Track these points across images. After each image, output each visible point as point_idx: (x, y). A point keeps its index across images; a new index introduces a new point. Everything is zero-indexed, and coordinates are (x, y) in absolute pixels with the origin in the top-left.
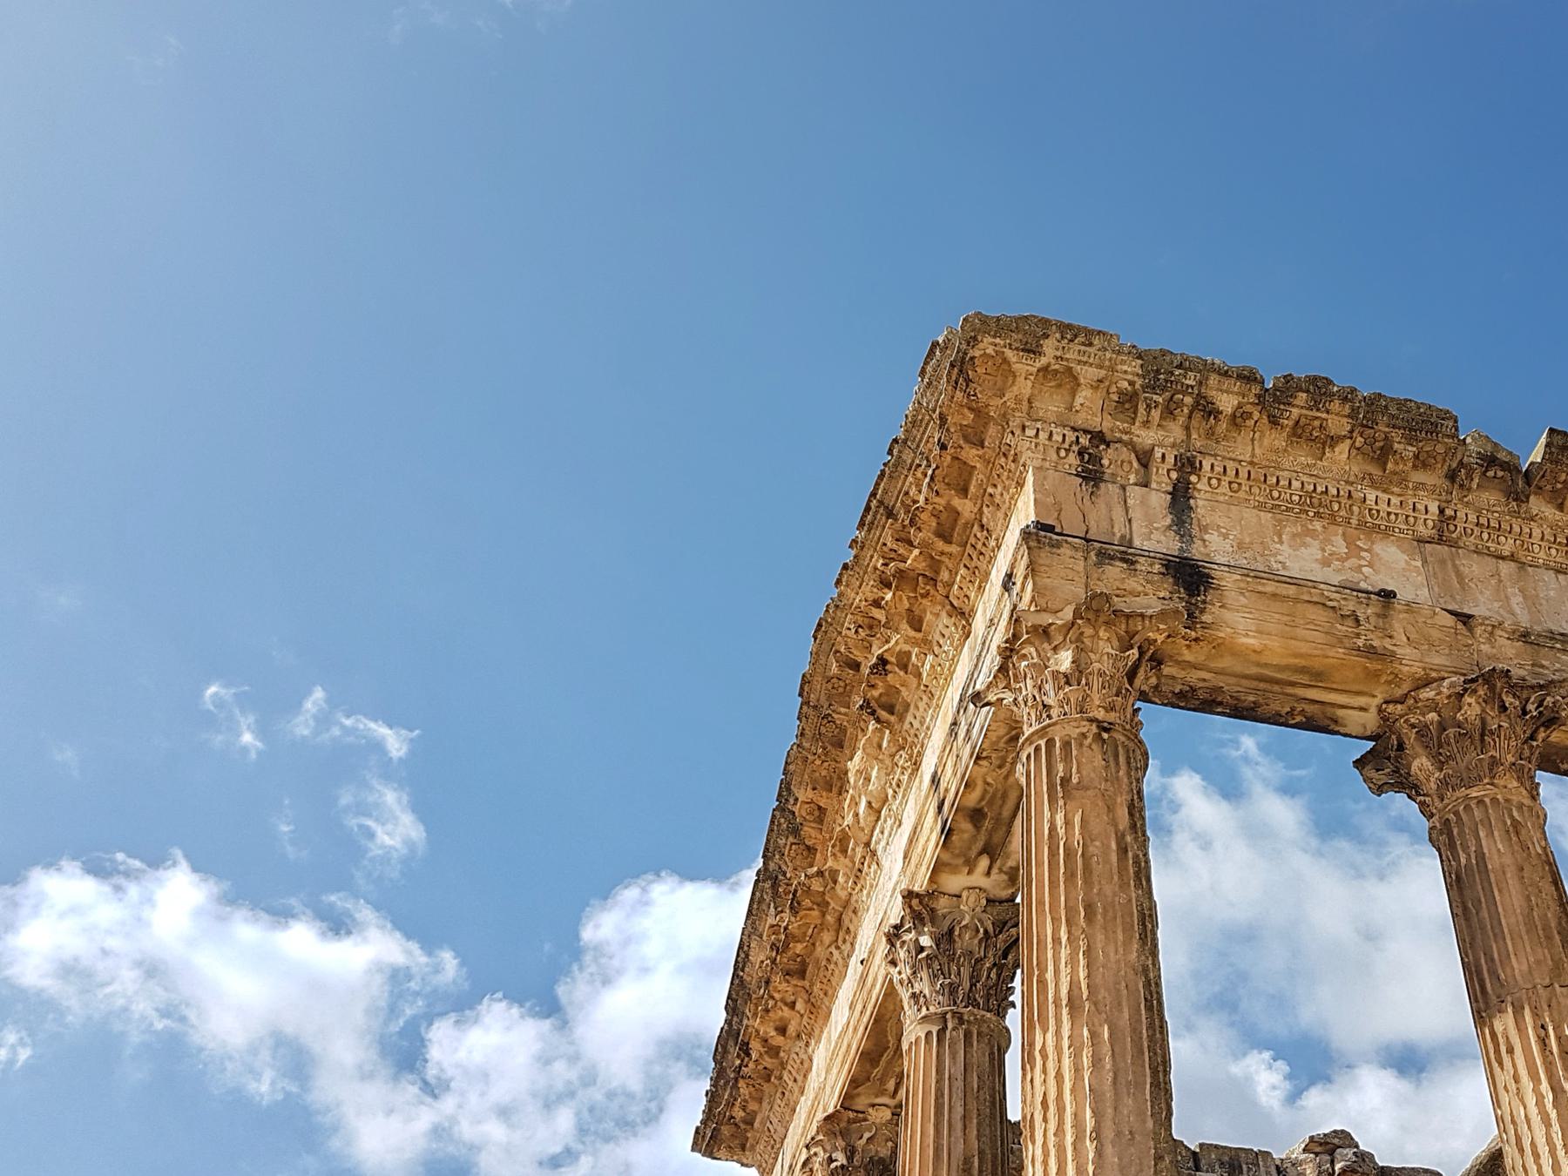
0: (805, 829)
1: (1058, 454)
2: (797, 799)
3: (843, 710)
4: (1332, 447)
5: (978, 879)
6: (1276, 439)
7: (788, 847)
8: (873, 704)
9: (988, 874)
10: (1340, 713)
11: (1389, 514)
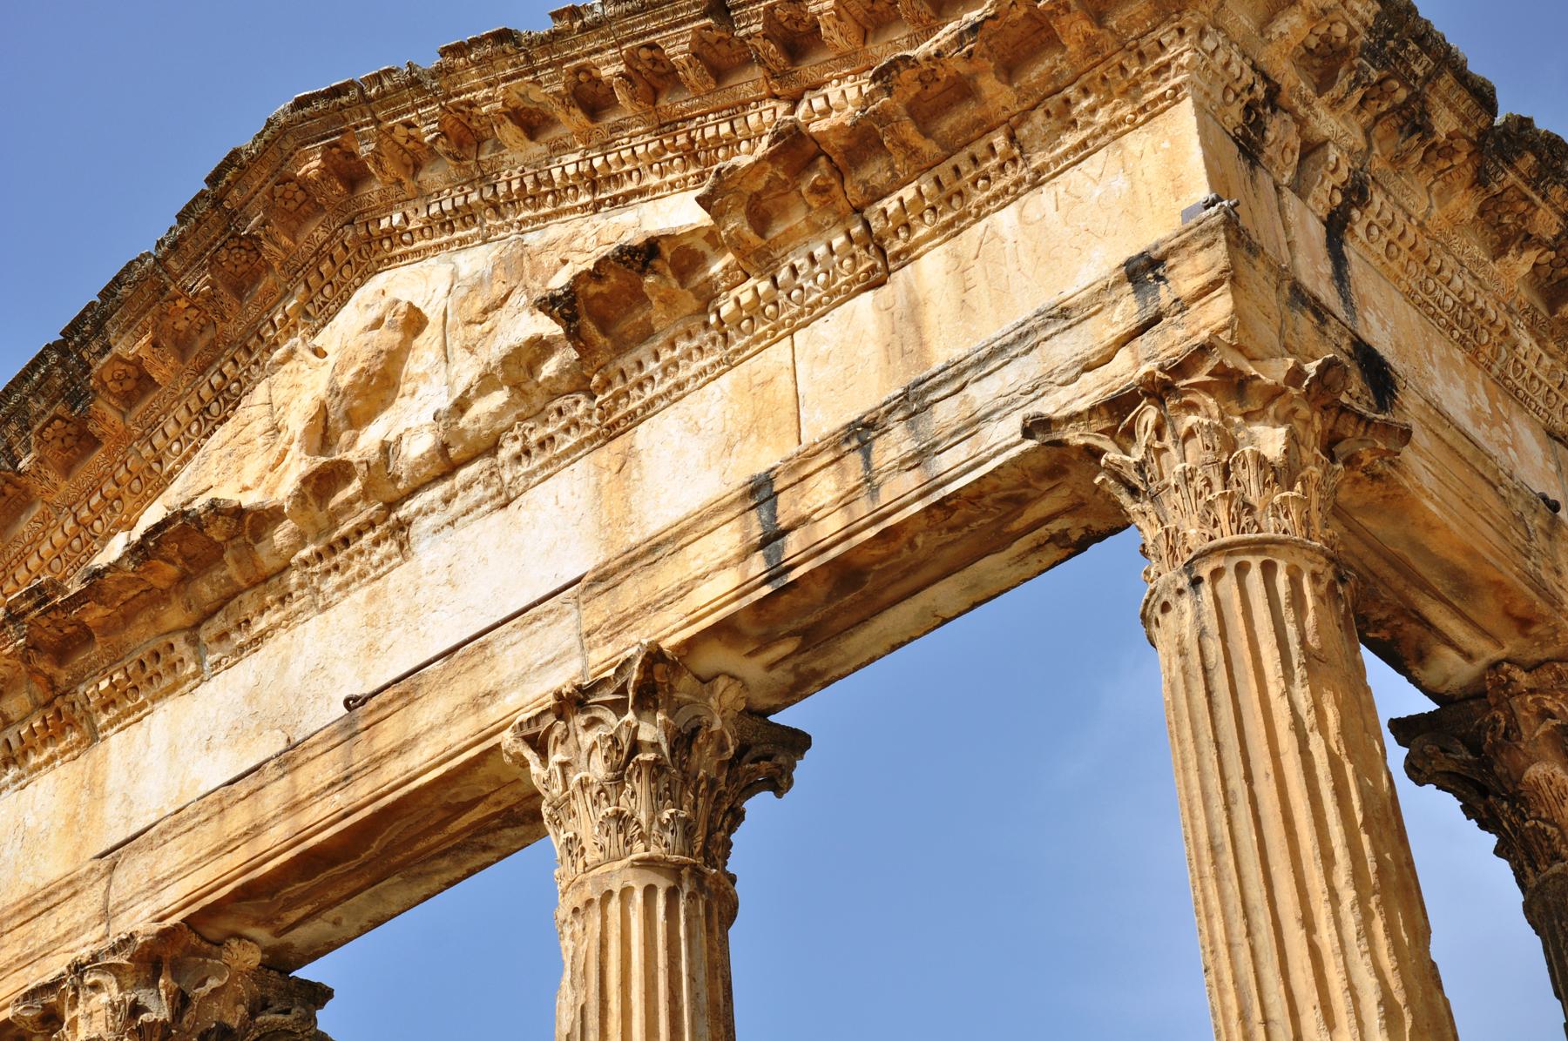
0: (100, 403)
1: (1224, 95)
2: (107, 348)
3: (285, 241)
4: (1522, 249)
5: (752, 669)
6: (1465, 204)
7: (45, 420)
8: (580, 304)
9: (771, 666)
11: (1533, 377)
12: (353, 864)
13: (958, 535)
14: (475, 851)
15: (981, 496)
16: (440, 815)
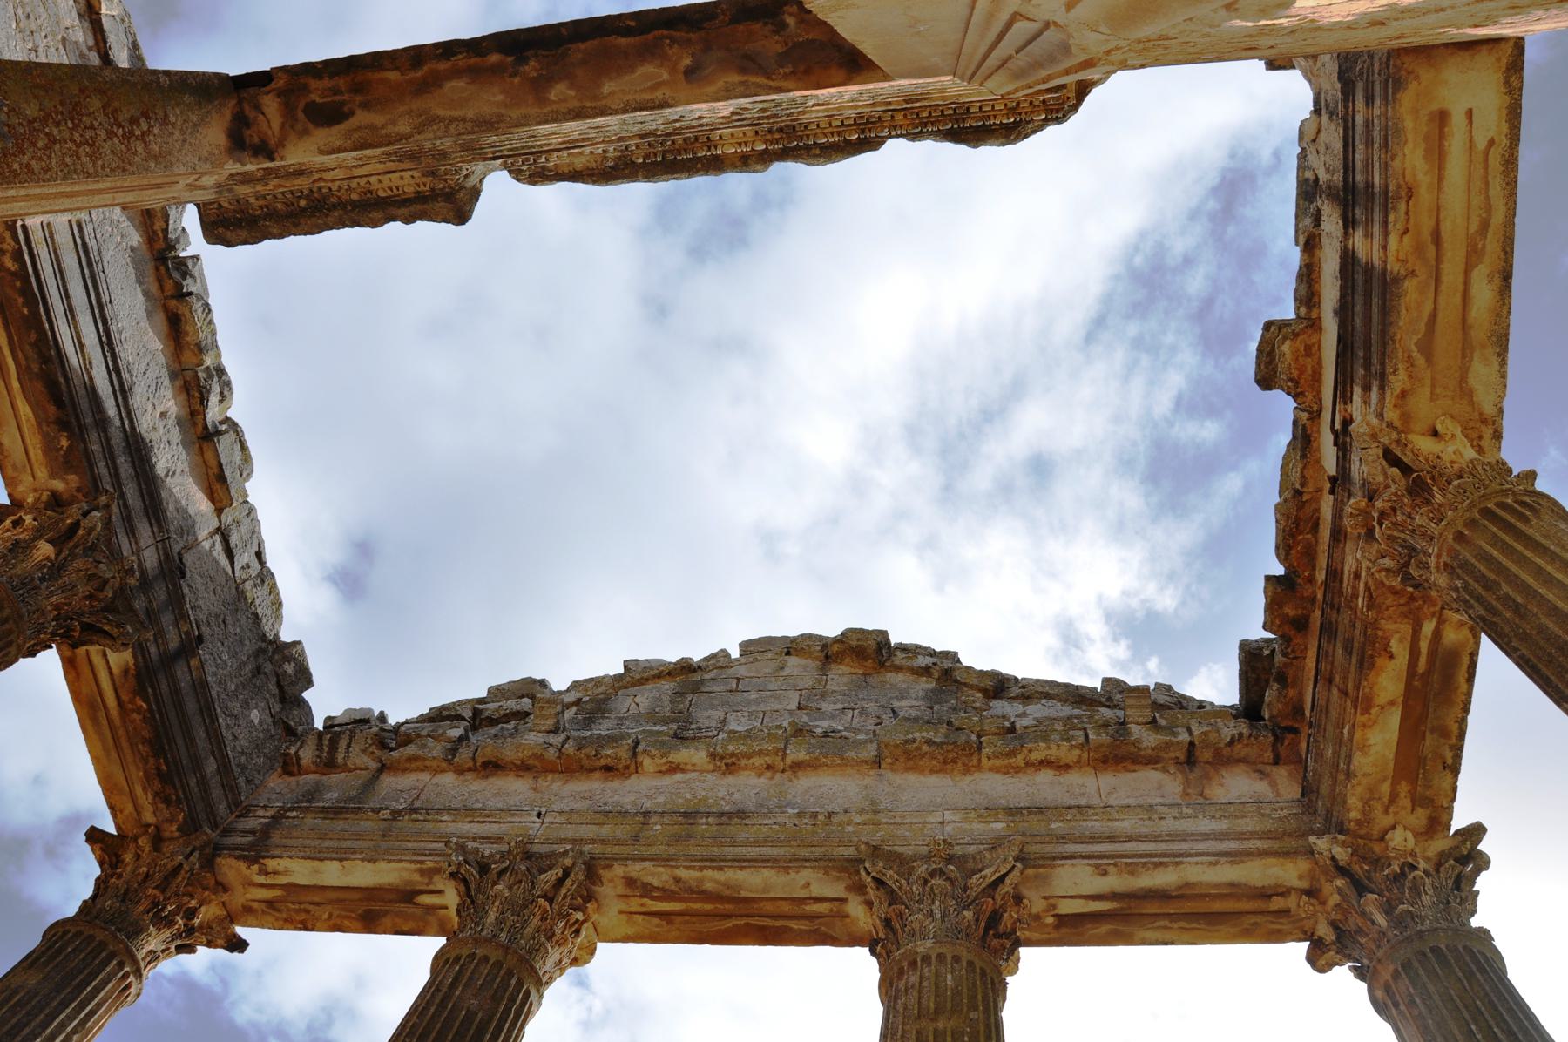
9: (440, 892)
10: (115, 670)
12: (751, 921)
13: (307, 906)
14: (685, 883)
15: (286, 920)
16: (678, 919)
